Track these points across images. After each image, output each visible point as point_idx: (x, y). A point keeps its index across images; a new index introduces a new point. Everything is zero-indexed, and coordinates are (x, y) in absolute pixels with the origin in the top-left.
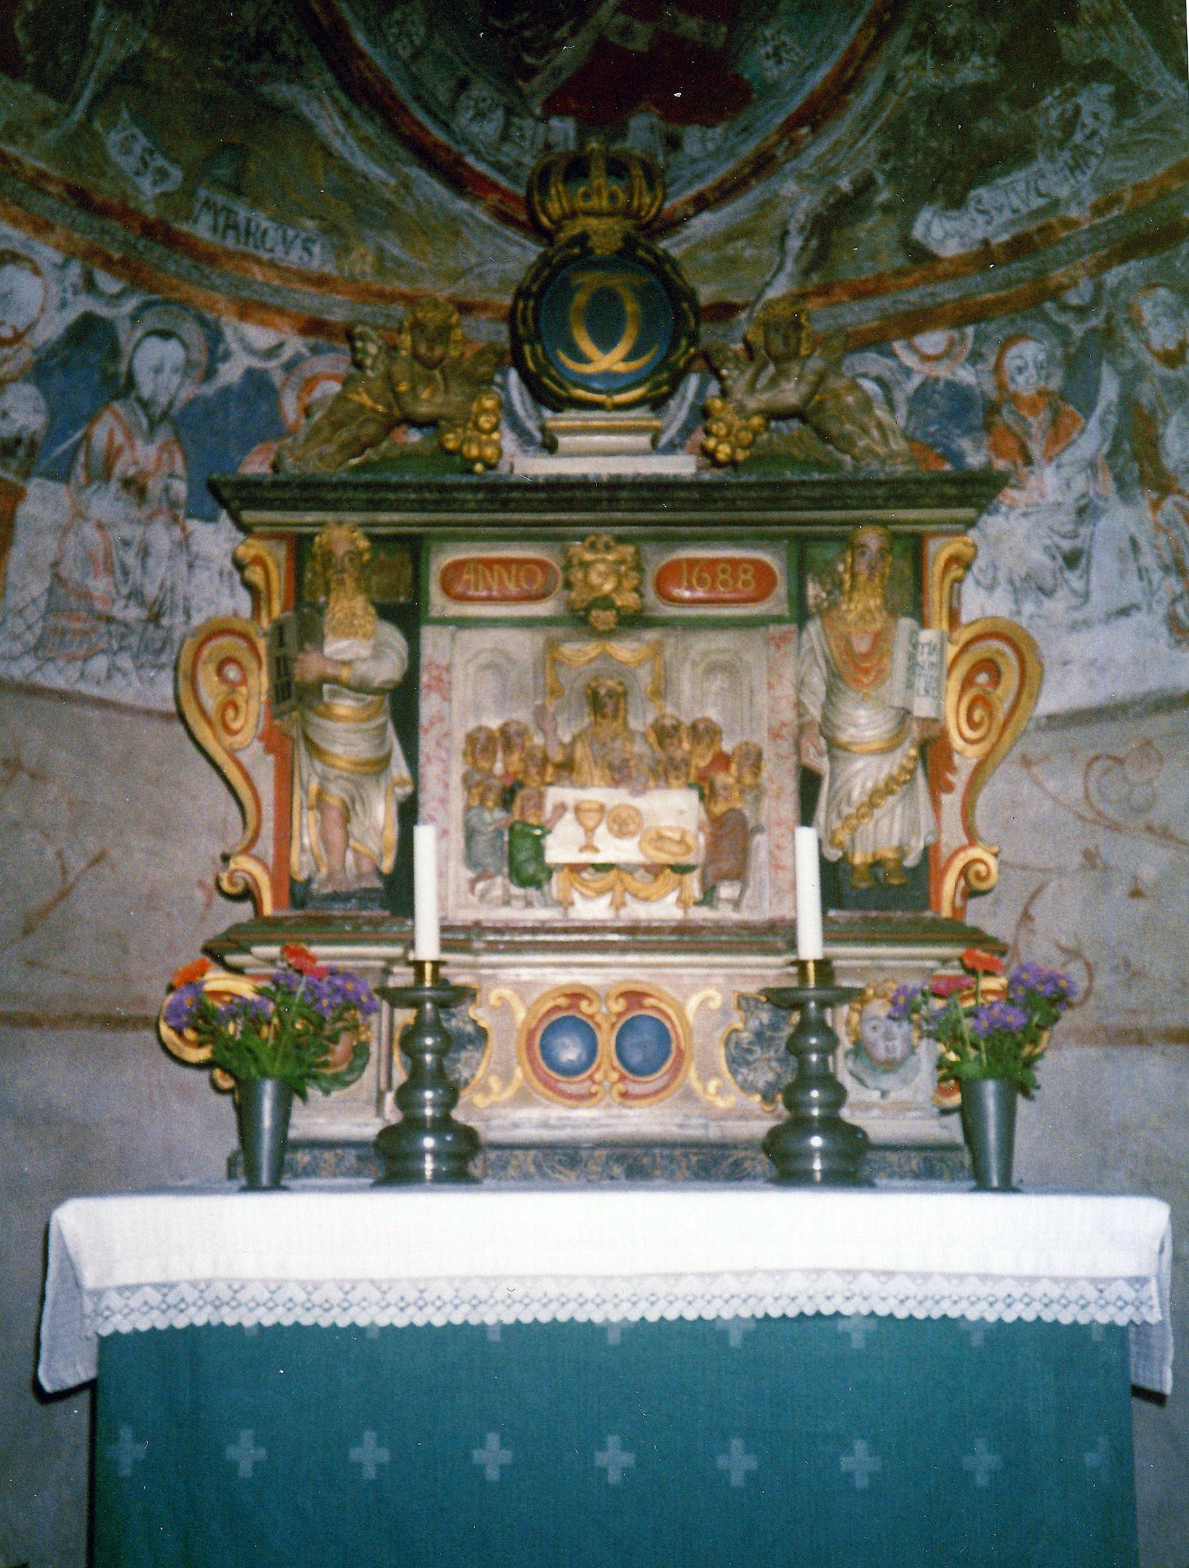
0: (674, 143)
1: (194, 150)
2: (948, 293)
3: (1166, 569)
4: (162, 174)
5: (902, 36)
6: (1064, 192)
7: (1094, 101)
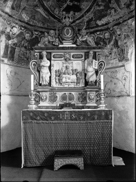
0: (75, 14)
1: (30, 16)
2: (100, 28)
3: (118, 55)
4: (27, 18)
5: (95, 4)
6: (110, 19)
7: (113, 11)
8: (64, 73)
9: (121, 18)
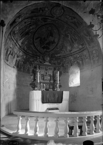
8: (46, 76)
9: (66, 55)
